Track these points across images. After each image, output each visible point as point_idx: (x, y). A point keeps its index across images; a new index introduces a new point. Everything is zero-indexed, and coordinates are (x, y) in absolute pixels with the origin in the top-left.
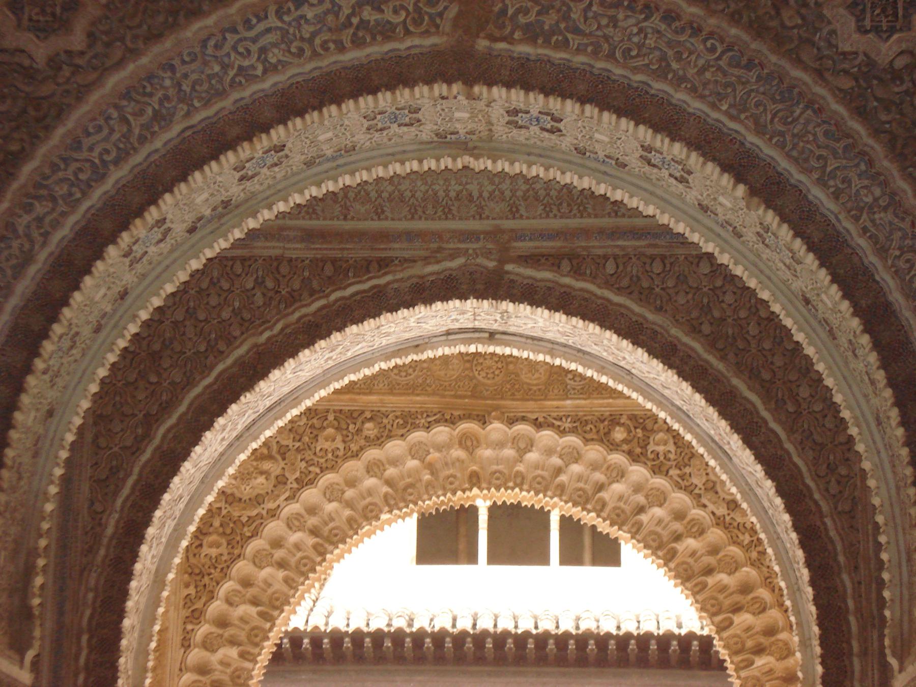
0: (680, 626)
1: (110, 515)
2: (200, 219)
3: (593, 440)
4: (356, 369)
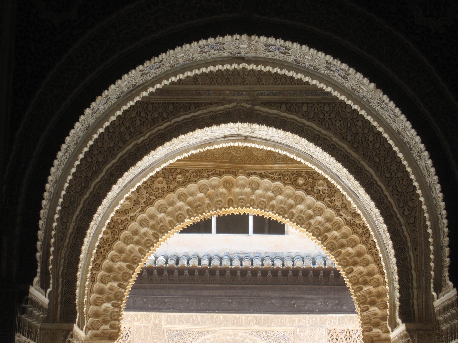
0: (314, 263)
1: (70, 224)
2: (122, 93)
3: (288, 183)
4: (180, 153)
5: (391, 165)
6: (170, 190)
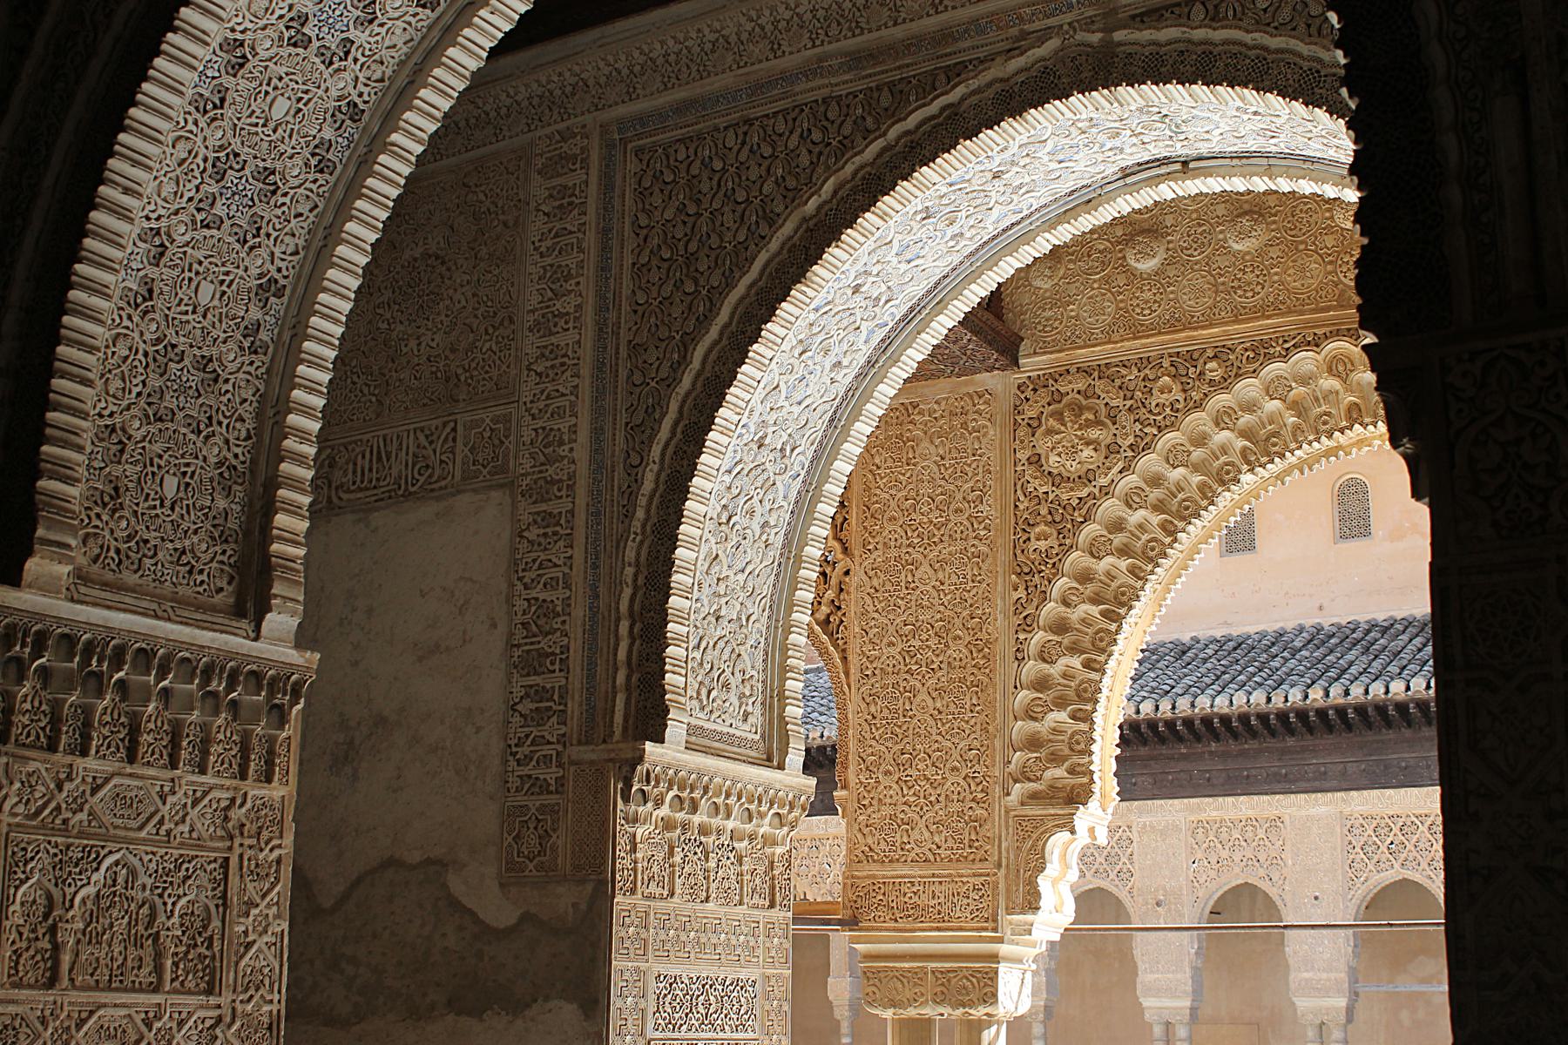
4: (1011, 249)
6: (1191, 404)
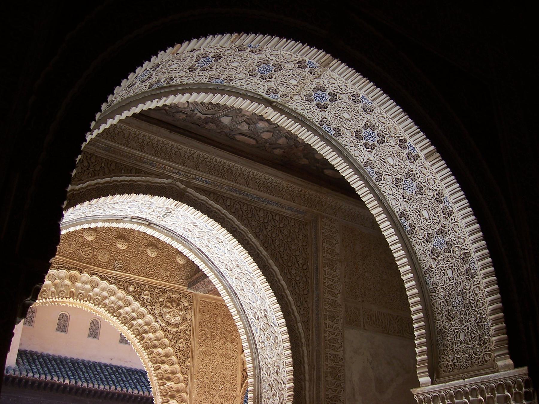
3: (121, 288)
5: (292, 269)
